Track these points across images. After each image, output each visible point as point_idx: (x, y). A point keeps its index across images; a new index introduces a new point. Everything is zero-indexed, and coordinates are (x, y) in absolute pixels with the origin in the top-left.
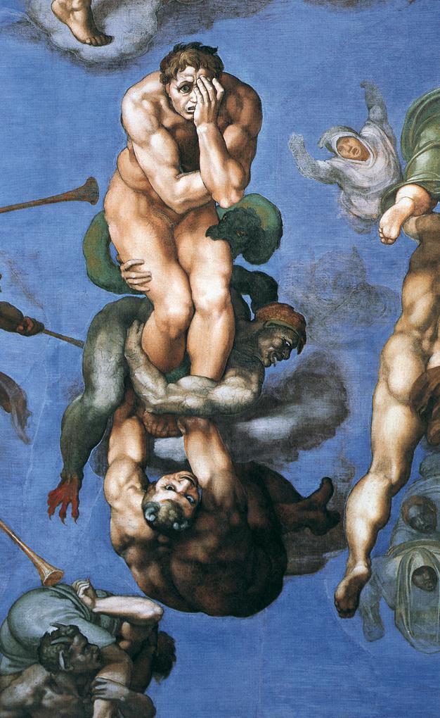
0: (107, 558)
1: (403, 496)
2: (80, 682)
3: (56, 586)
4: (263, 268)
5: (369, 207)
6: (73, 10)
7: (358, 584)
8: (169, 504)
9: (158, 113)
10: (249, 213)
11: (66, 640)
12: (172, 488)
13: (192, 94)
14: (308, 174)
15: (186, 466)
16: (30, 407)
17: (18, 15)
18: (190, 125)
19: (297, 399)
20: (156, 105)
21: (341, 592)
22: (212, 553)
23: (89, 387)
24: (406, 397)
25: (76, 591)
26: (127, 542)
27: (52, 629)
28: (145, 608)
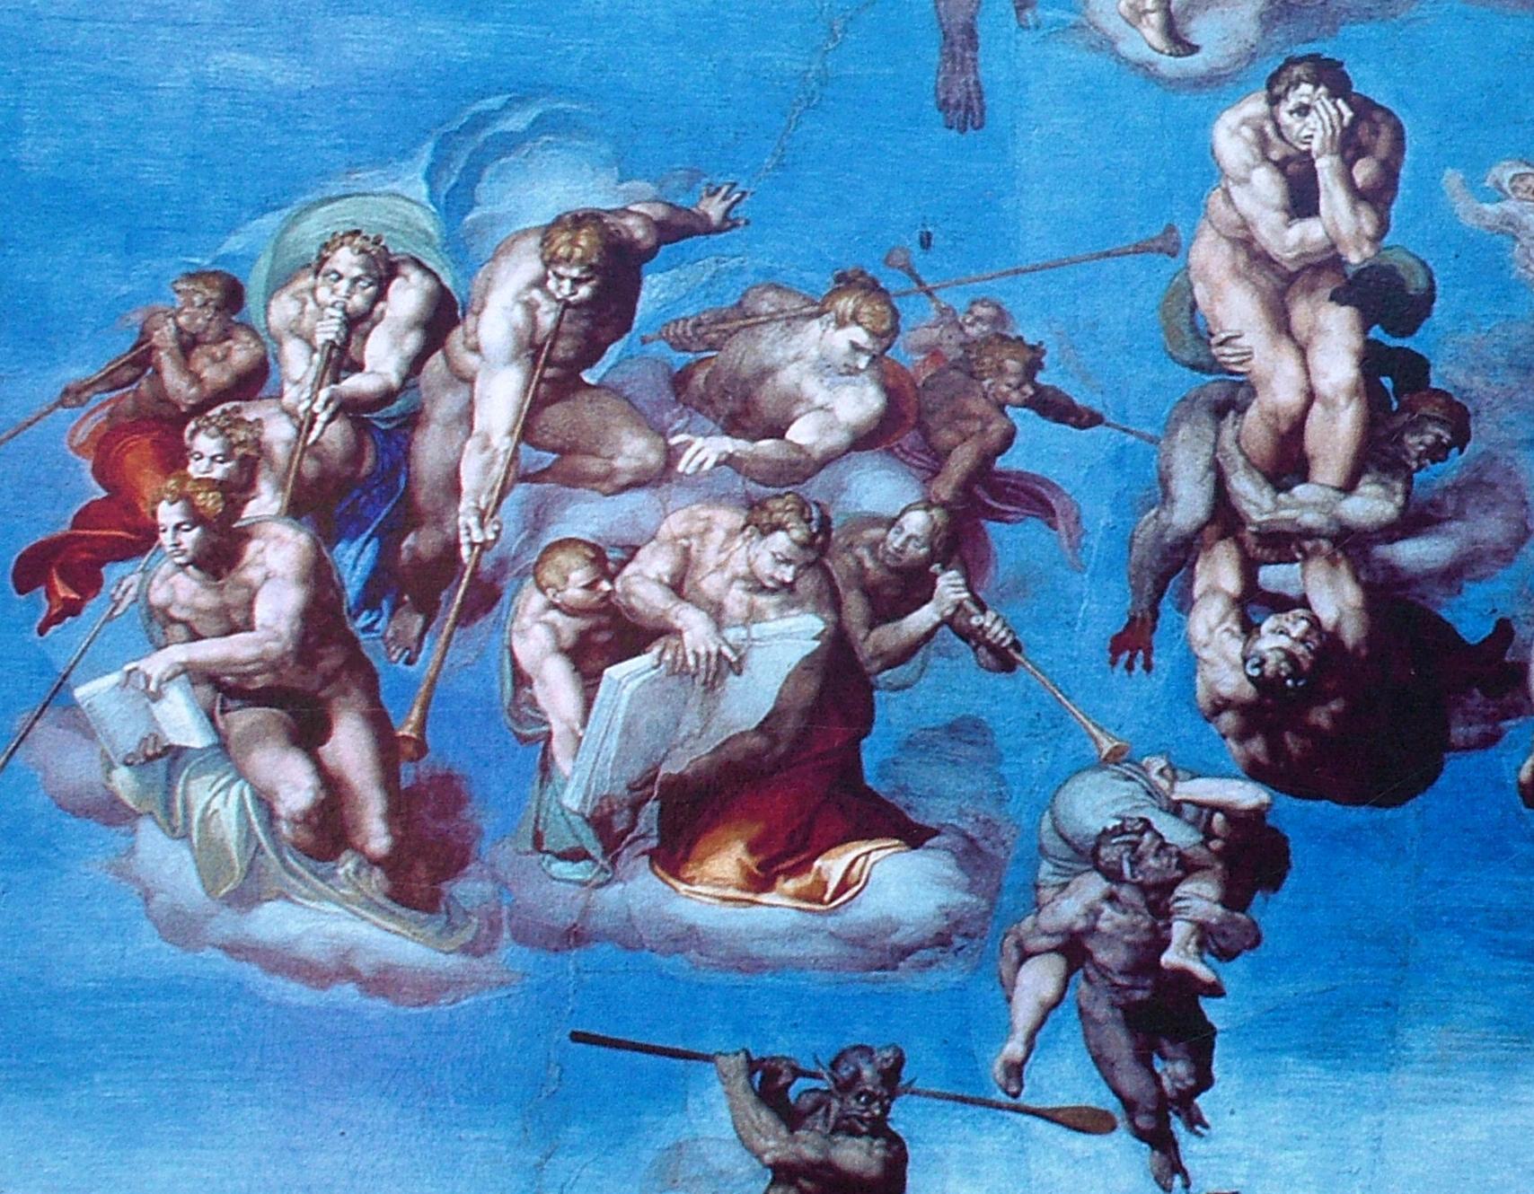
0: (1189, 726)
2: (1152, 897)
4: (1407, 343)
6: (1146, 12)
8: (1281, 655)
9: (1263, 143)
10: (1391, 271)
11: (1134, 838)
13: (1308, 119)
14: (1469, 221)
15: (1304, 602)
17: (1073, 18)
18: (1307, 159)
19: (1459, 515)
20: (1260, 132)
23: (1166, 497)
25: (1145, 770)
26: (1221, 705)
27: (1111, 824)
28: (1247, 795)
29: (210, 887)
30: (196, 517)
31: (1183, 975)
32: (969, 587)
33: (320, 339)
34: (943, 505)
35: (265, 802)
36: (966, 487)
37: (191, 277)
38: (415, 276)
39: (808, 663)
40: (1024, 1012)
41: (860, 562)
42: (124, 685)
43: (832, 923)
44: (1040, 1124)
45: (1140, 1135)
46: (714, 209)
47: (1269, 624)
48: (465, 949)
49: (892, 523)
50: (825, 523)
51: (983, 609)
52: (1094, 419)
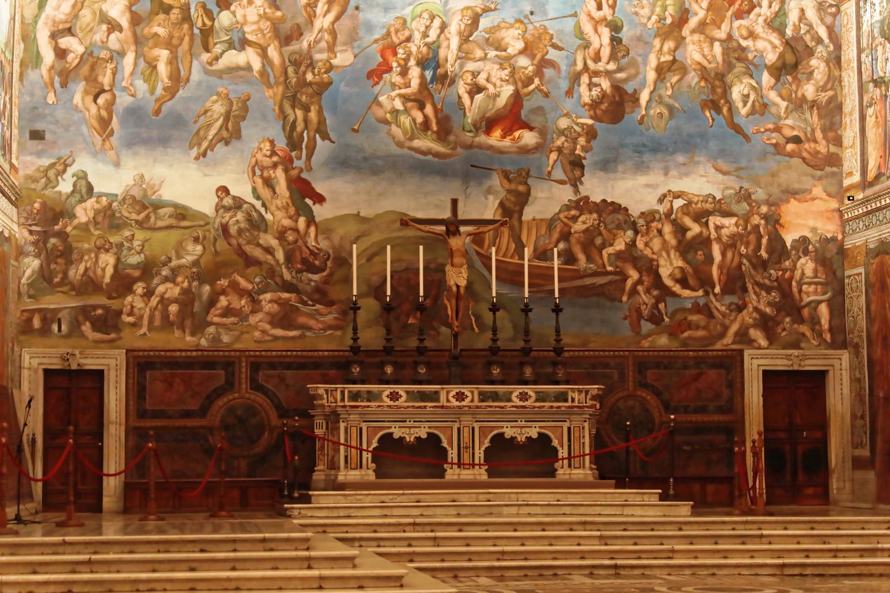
0: (580, 109)
1: (654, 94)
3: (567, 115)
5: (644, 20)
7: (643, 117)
10: (615, 21)
14: (629, 12)
15: (600, 85)
21: (639, 118)
22: (606, 108)
23: (575, 64)
26: (585, 104)
28: (590, 122)
29: (405, 137)
30: (399, 65)
31: (579, 155)
32: (540, 81)
33: (421, 31)
35: (414, 120)
37: (396, 18)
38: (438, 18)
39: (512, 95)
40: (551, 162)
42: (388, 98)
43: (517, 145)
44: (554, 183)
45: (571, 185)
46: (493, 6)
47: (594, 89)
48: (450, 149)
49: (526, 68)
50: (514, 68)
51: (543, 85)
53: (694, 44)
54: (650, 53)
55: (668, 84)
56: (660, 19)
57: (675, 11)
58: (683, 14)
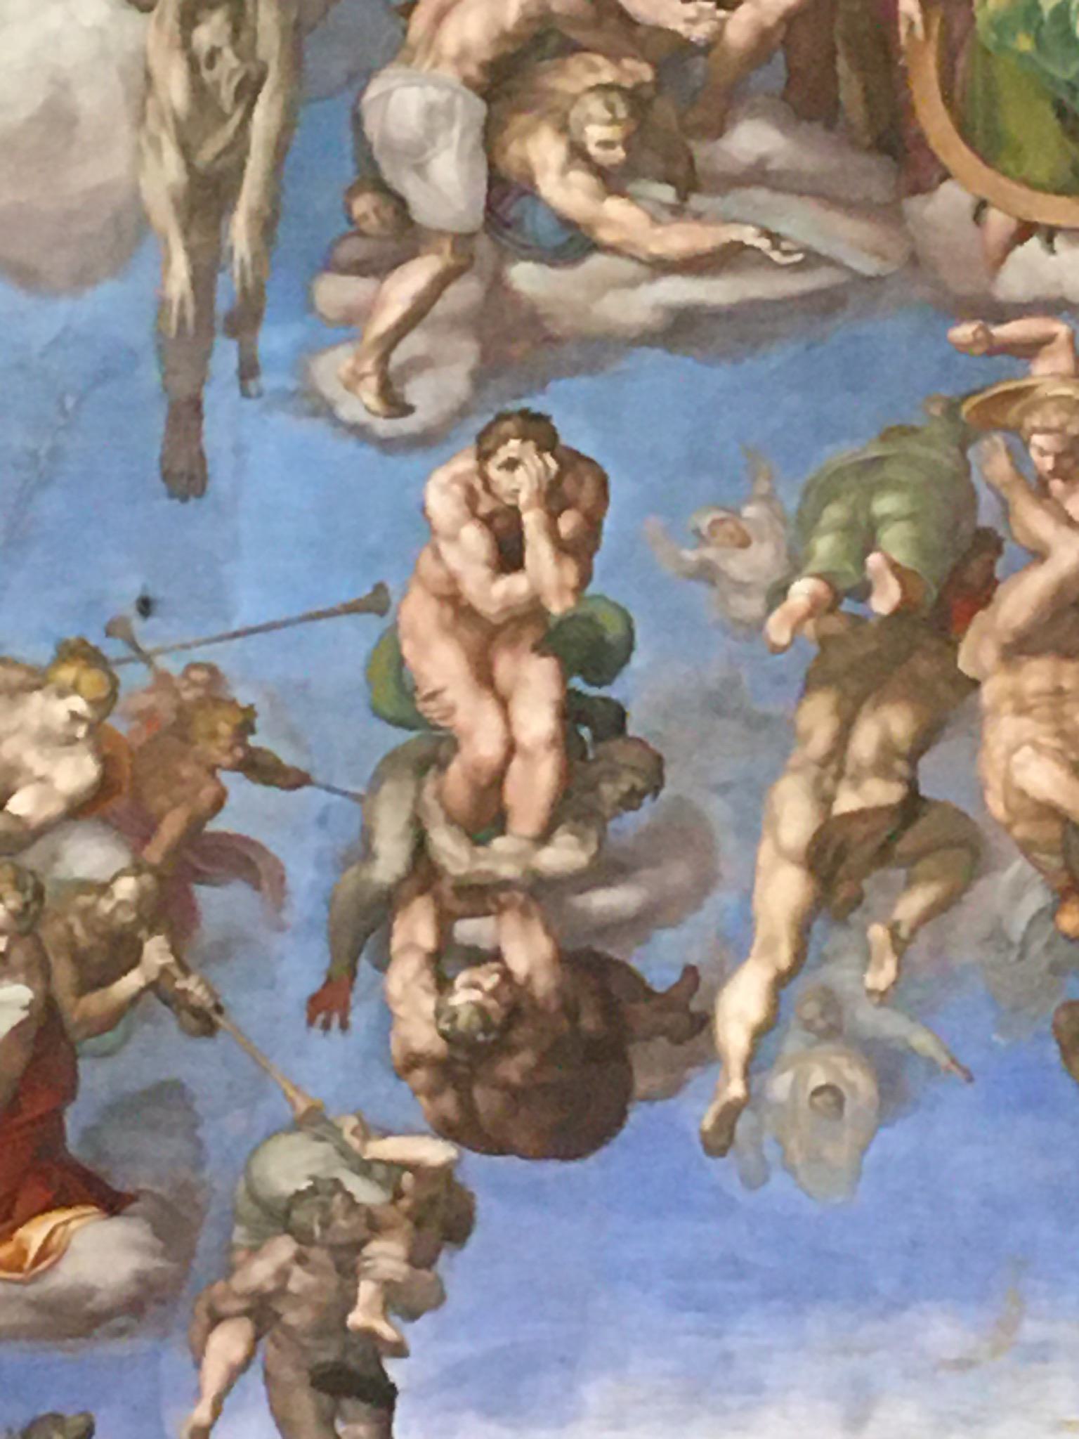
0: (384, 1085)
5: (752, 606)
7: (730, 1113)
8: (471, 1008)
9: (471, 499)
10: (590, 620)
12: (476, 986)
16: (290, 883)
17: (291, 385)
18: (514, 514)
21: (708, 1122)
22: (528, 1073)
23: (366, 852)
24: (802, 858)
25: (339, 1131)
26: (413, 1062)
27: (304, 1185)
28: (435, 1152)
31: (370, 1335)
32: (173, 951)
34: (153, 869)
36: (174, 852)
39: (16, 1030)
40: (213, 1374)
41: (70, 929)
43: (32, 1291)
47: (463, 978)
49: (104, 889)
50: (39, 893)
51: (186, 971)
52: (298, 780)
53: (1022, 710)
54: (775, 774)
55: (878, 932)
56: (837, 597)
57: (920, 546)
58: (965, 559)
